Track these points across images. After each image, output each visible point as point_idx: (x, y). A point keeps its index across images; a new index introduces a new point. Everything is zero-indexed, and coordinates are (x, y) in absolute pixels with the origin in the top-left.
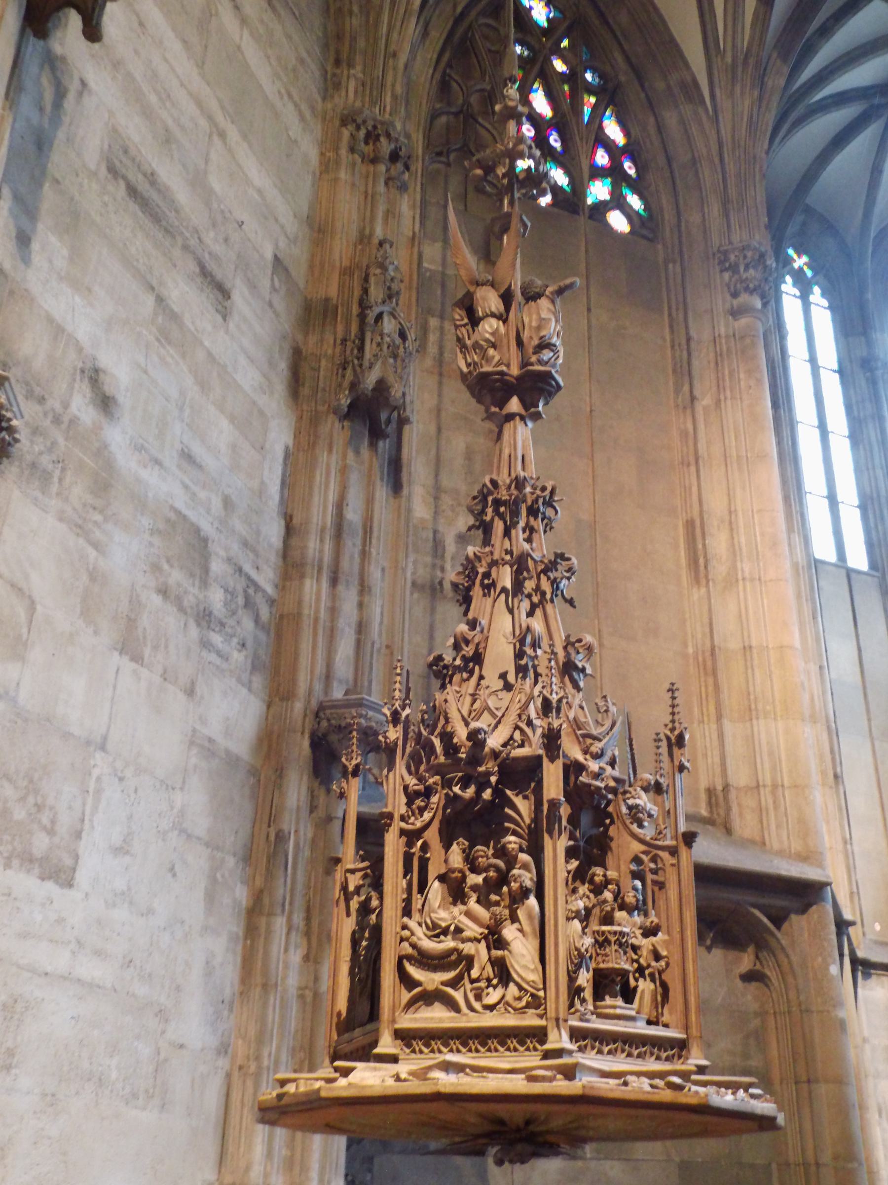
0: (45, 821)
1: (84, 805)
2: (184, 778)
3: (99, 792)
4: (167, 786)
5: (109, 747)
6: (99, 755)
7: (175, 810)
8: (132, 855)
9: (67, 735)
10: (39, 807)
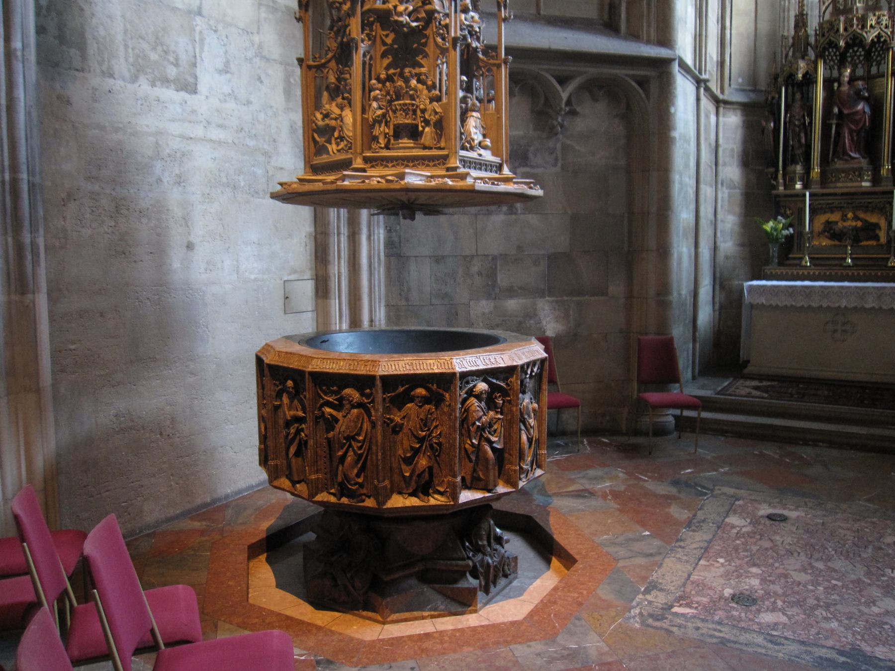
0: (172, 59)
1: (194, 48)
2: (258, 26)
3: (202, 40)
4: (247, 32)
5: (204, 12)
6: (198, 19)
7: (256, 46)
8: (231, 73)
9: (174, 9)
10: (166, 52)
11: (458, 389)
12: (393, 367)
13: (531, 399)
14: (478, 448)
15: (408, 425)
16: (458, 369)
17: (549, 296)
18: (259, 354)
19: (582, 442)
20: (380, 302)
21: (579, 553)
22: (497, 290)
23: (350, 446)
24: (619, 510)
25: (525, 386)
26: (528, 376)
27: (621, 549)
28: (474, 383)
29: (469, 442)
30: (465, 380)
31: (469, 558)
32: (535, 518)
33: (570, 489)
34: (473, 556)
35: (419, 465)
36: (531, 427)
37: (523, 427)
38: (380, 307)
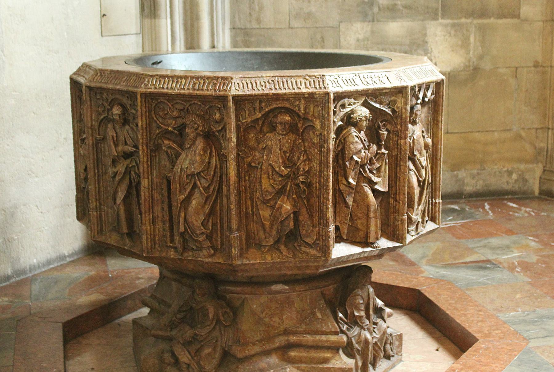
11: (332, 113)
12: (250, 86)
13: (423, 132)
14: (358, 190)
15: (268, 160)
16: (332, 89)
17: (443, 18)
18: (75, 77)
19: (483, 207)
20: (224, 24)
21: (480, 332)
22: (376, 10)
23: (195, 186)
24: (530, 283)
25: (416, 115)
26: (419, 101)
27: (533, 327)
28: (351, 108)
29: (345, 183)
30: (340, 103)
31: (342, 332)
32: (422, 291)
33: (468, 259)
34: (347, 329)
35: (283, 212)
36: (423, 167)
37: (412, 167)
38: (223, 30)
